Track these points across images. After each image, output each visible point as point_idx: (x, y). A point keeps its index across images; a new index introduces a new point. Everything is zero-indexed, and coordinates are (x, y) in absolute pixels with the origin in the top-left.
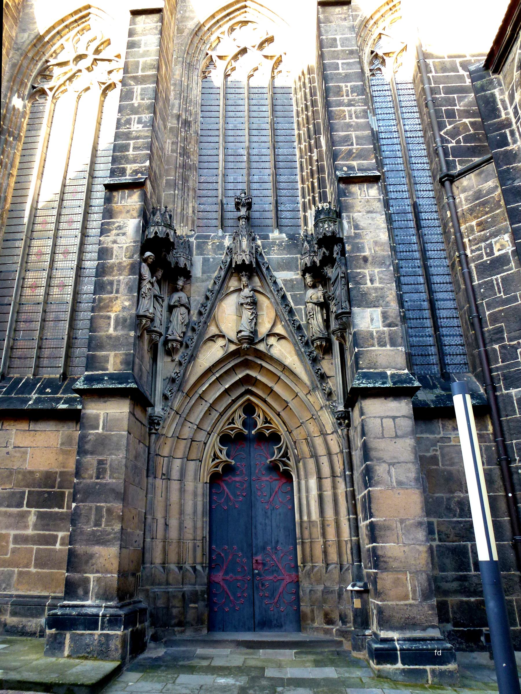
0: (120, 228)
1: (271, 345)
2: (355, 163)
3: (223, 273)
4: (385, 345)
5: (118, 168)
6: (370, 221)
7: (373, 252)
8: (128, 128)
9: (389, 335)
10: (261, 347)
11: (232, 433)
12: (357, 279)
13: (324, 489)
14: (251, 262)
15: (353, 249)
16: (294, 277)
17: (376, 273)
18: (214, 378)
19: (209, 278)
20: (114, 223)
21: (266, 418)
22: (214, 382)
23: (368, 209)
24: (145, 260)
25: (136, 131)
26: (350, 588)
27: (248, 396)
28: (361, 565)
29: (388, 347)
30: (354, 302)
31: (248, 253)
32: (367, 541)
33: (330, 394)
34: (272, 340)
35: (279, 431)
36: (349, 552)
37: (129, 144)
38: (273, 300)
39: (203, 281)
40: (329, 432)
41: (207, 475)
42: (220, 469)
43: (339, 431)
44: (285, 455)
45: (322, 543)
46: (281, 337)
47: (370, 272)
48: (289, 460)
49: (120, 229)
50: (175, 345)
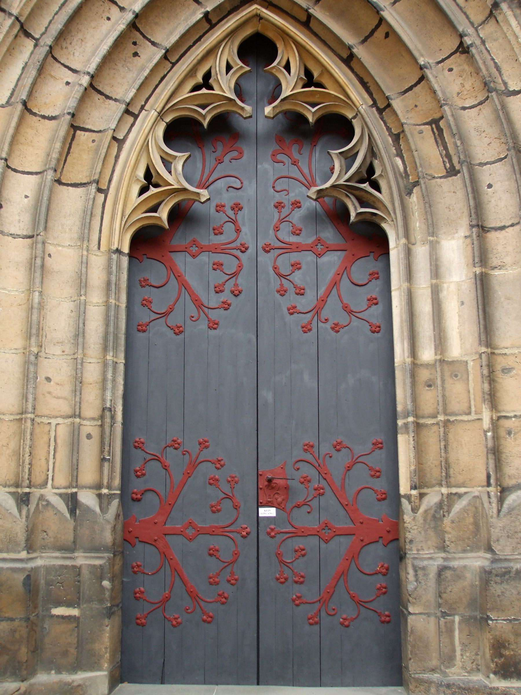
11: (203, 112)
13: (494, 261)
21: (308, 73)
35: (350, 103)
41: (124, 230)
42: (164, 213)
45: (486, 423)
48: (376, 186)
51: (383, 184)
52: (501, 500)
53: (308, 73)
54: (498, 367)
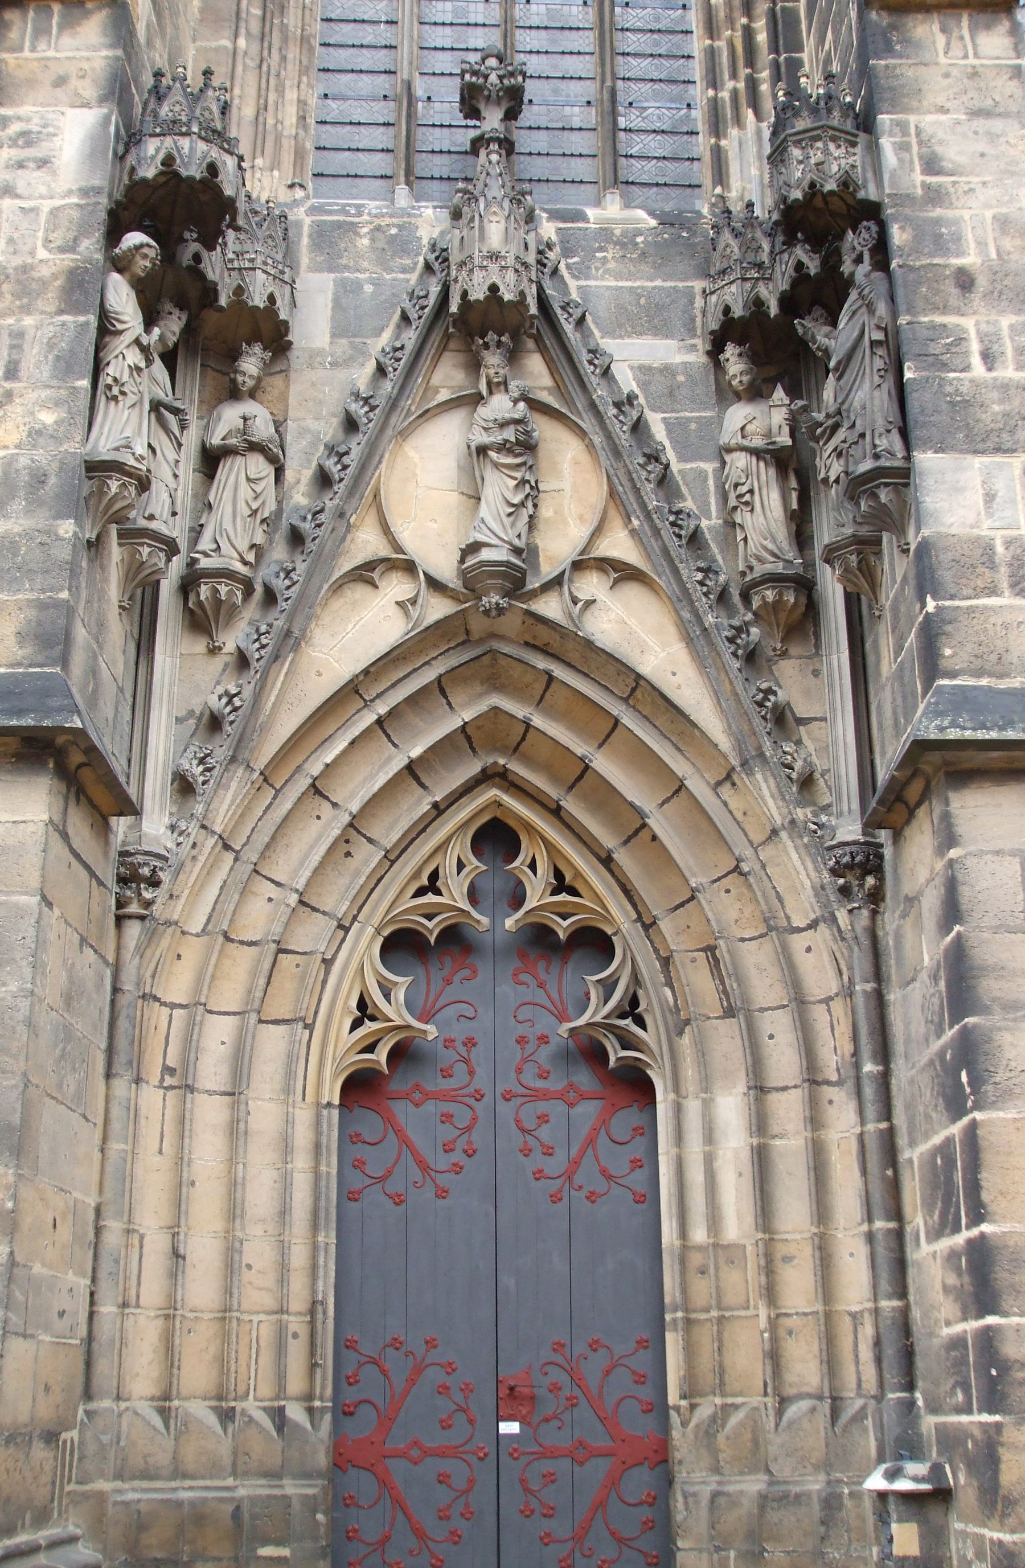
1: (590, 603)
3: (411, 337)
6: (981, 146)
7: (993, 255)
10: (550, 607)
11: (430, 925)
13: (775, 1128)
14: (522, 294)
15: (918, 238)
16: (678, 359)
17: (1005, 332)
18: (369, 718)
19: (361, 352)
21: (559, 875)
22: (366, 733)
23: (977, 104)
26: (876, 1482)
27: (492, 793)
28: (912, 1403)
31: (510, 261)
32: (947, 1308)
33: (807, 782)
35: (609, 920)
36: (866, 1353)
38: (598, 440)
39: (334, 364)
40: (798, 922)
41: (335, 1076)
42: (381, 1056)
43: (842, 917)
44: (631, 1008)
45: (763, 1322)
47: (984, 327)
48: (640, 1022)
51: (648, 1020)
52: (780, 1413)
53: (559, 875)
54: (778, 1256)
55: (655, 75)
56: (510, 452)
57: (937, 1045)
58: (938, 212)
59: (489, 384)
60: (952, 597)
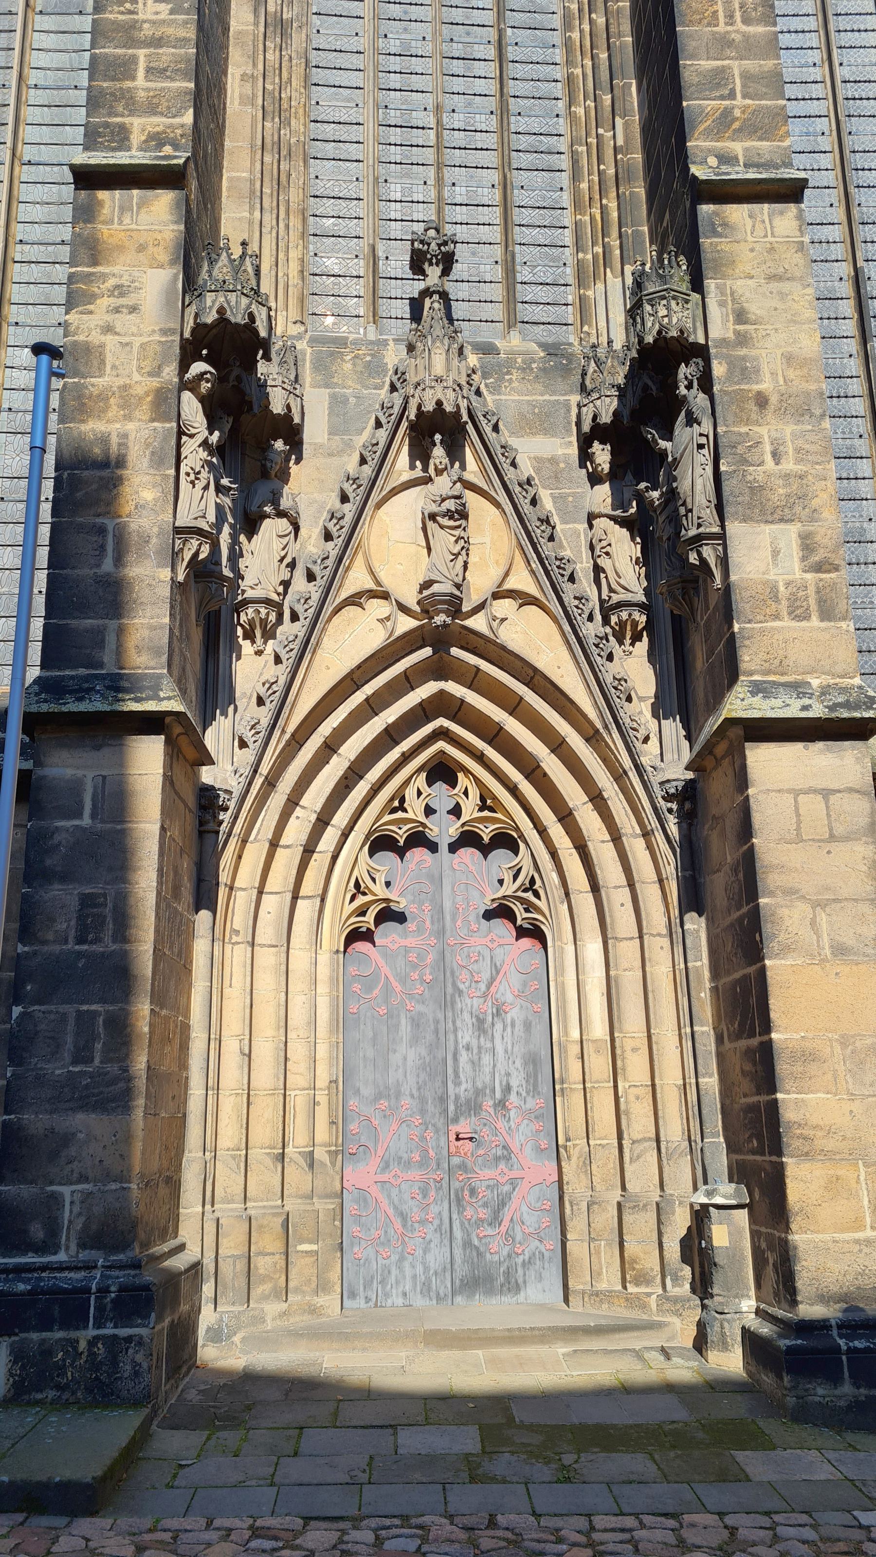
0: (120, 290)
2: (738, 148)
4: (807, 617)
5: (107, 125)
6: (775, 303)
7: (781, 382)
8: (131, 12)
9: (818, 592)
10: (478, 623)
12: (740, 450)
14: (458, 406)
15: (730, 372)
16: (560, 452)
17: (788, 437)
19: (349, 445)
20: (104, 277)
24: (192, 386)
25: (154, 23)
29: (815, 621)
30: (728, 510)
31: (450, 383)
34: (504, 607)
37: (134, 59)
39: (331, 455)
46: (525, 600)
47: (774, 434)
48: (537, 895)
49: (122, 295)
50: (263, 611)
53: (483, 799)
55: (542, 241)
56: (451, 518)
57: (736, 915)
58: (743, 352)
59: (436, 469)
60: (750, 622)
